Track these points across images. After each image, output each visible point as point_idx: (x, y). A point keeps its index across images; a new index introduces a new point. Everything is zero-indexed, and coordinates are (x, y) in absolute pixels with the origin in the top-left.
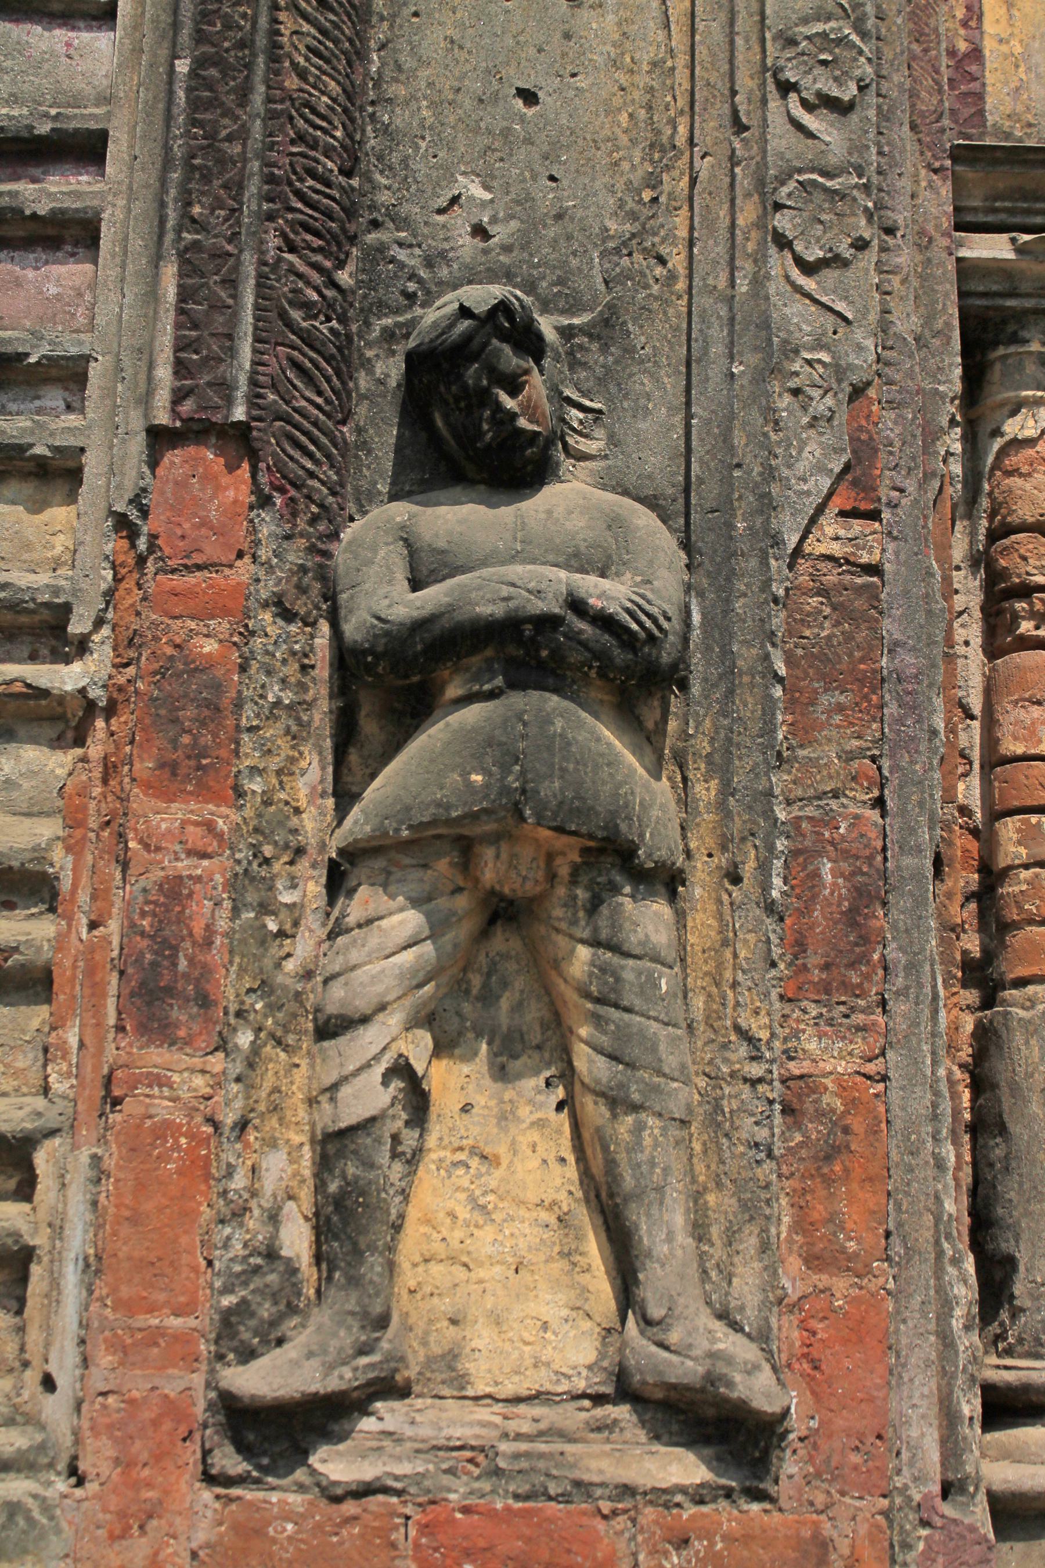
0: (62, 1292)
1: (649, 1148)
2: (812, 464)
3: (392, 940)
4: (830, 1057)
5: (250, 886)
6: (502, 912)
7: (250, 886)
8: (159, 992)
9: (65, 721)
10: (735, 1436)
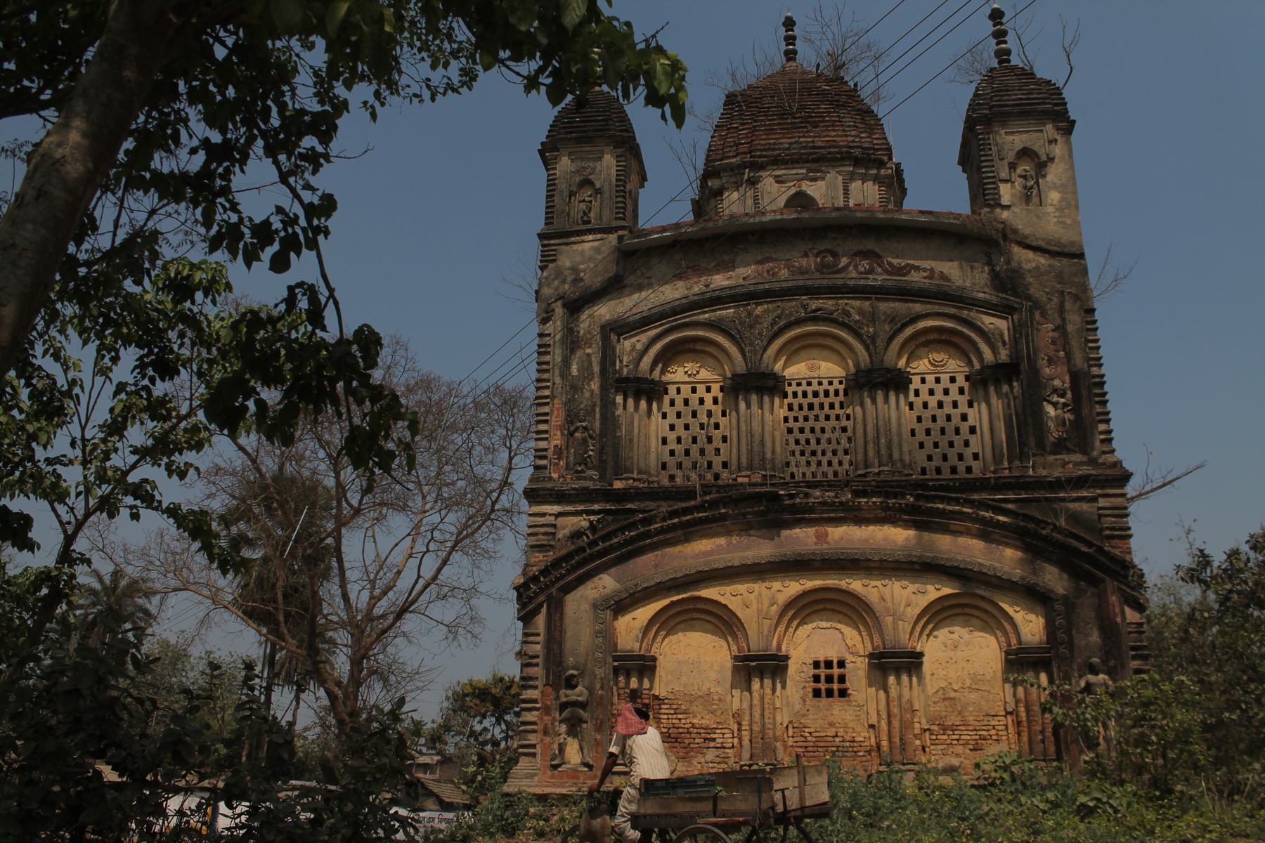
0: (539, 757)
1: (584, 744)
2: (598, 686)
3: (564, 728)
4: (598, 737)
5: (553, 724)
6: (573, 725)
7: (553, 724)
8: (546, 733)
9: (537, 709)
10: (590, 767)
